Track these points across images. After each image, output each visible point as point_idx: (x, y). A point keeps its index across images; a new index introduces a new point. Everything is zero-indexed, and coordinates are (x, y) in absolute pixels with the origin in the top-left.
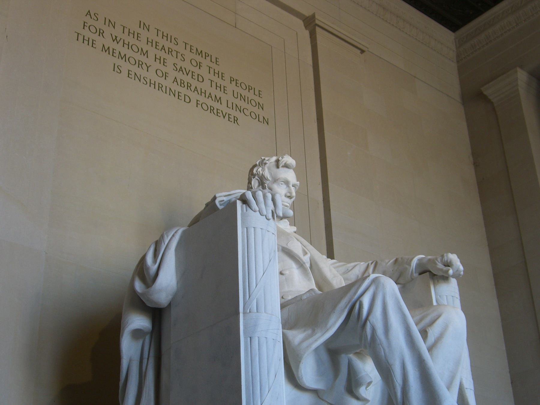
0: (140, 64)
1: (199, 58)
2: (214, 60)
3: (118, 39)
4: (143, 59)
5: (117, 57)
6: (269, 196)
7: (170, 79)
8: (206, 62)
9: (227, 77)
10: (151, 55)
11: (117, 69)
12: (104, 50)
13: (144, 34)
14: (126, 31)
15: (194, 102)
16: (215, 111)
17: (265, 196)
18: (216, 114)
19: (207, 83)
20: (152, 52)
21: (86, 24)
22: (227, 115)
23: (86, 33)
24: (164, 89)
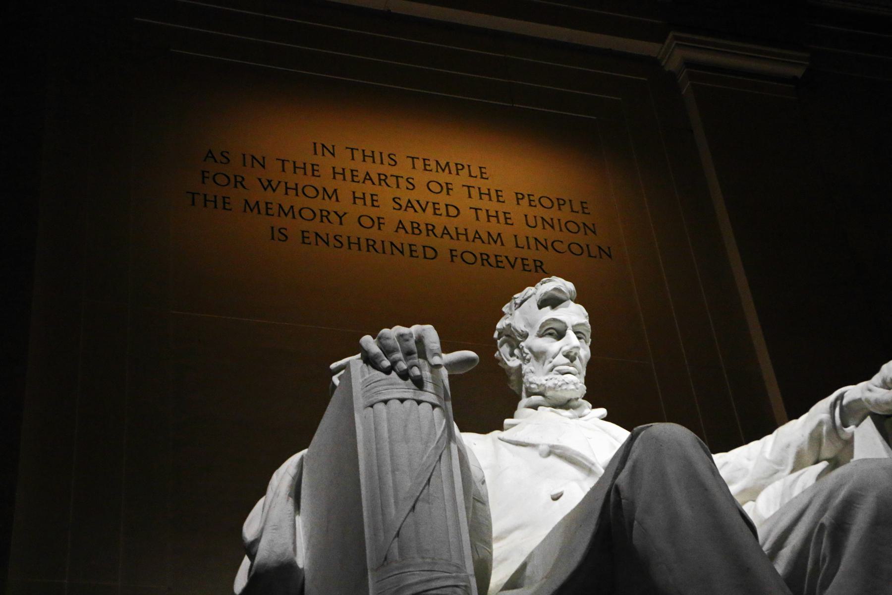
0: (325, 216)
1: (443, 177)
2: (475, 172)
3: (274, 184)
4: (330, 205)
5: (276, 214)
8: (458, 181)
9: (508, 196)
12: (248, 209)
13: (326, 163)
15: (444, 254)
16: (492, 260)
18: (495, 265)
20: (345, 189)
21: (206, 175)
22: (519, 261)
24: (378, 246)
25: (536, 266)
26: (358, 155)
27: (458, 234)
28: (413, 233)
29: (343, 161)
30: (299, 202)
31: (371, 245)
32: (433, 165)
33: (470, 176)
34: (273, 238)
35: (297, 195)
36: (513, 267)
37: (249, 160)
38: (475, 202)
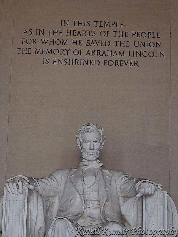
0: (62, 52)
1: (106, 29)
2: (119, 25)
3: (46, 41)
6: (15, 184)
7: (84, 52)
8: (111, 30)
9: (130, 34)
10: (70, 42)
11: (46, 61)
13: (64, 28)
14: (52, 32)
15: (102, 63)
16: (119, 63)
17: (13, 185)
19: (113, 44)
20: (70, 38)
21: (24, 40)
23: (25, 46)
24: (79, 62)
25: (135, 64)
26: (77, 23)
27: (108, 53)
28: (92, 55)
29: (71, 27)
30: (53, 47)
31: (77, 61)
32: (103, 23)
33: (117, 27)
34: (44, 64)
35: (53, 44)
36: (126, 65)
37: (38, 31)
38: (117, 38)
